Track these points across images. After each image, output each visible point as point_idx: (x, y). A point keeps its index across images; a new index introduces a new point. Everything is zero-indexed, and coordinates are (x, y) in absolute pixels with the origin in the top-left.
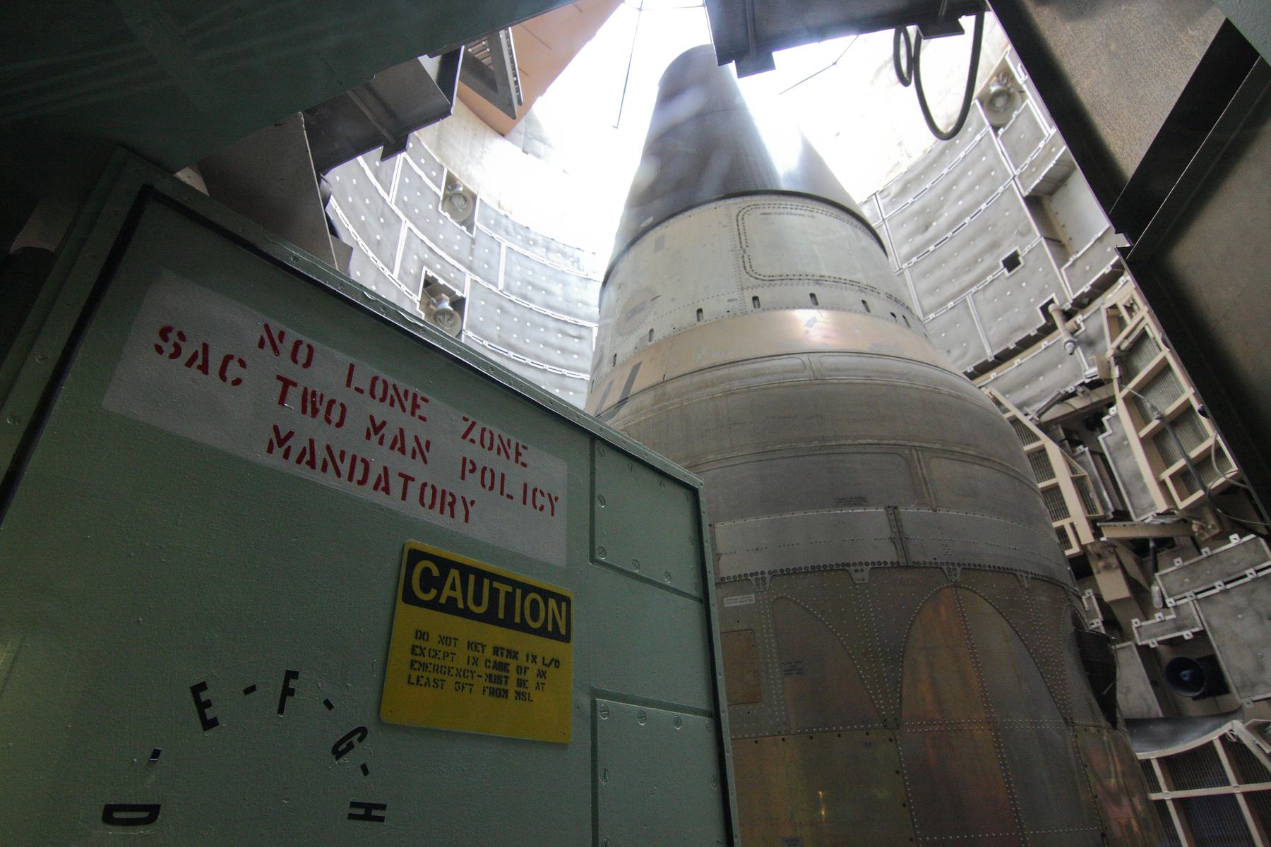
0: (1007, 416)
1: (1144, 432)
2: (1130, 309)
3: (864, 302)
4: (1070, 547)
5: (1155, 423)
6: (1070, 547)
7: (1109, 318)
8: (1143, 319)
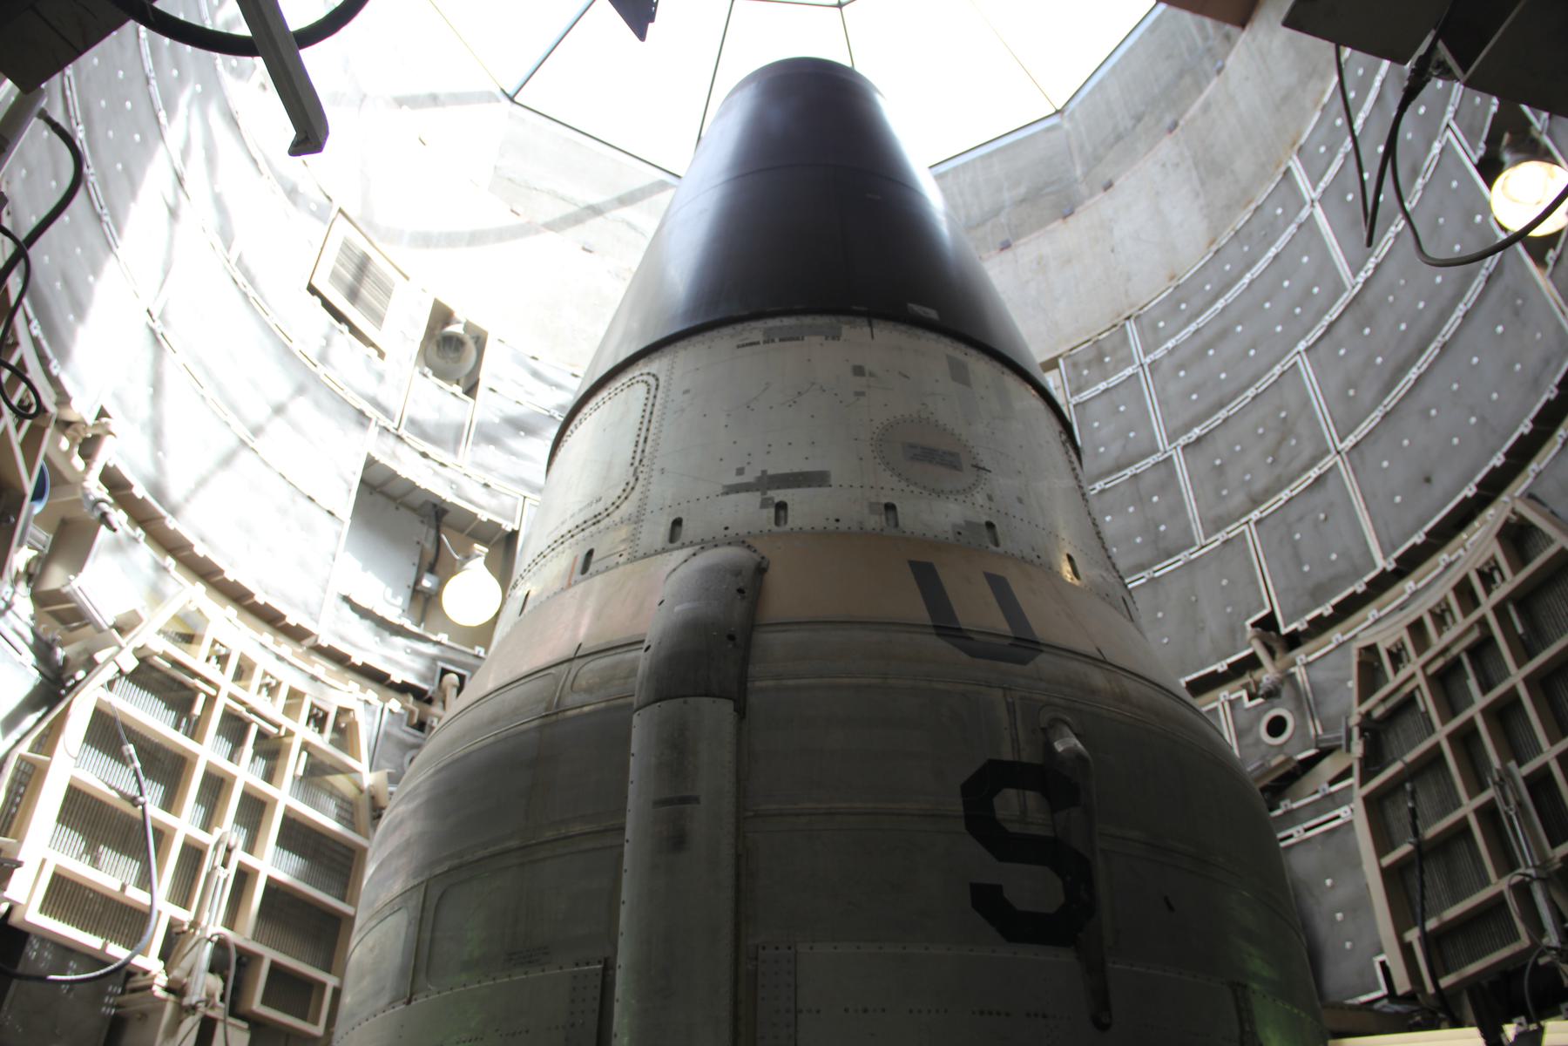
1: (1388, 860)
2: (1397, 657)
5: (1405, 849)
7: (1361, 664)
8: (1412, 676)
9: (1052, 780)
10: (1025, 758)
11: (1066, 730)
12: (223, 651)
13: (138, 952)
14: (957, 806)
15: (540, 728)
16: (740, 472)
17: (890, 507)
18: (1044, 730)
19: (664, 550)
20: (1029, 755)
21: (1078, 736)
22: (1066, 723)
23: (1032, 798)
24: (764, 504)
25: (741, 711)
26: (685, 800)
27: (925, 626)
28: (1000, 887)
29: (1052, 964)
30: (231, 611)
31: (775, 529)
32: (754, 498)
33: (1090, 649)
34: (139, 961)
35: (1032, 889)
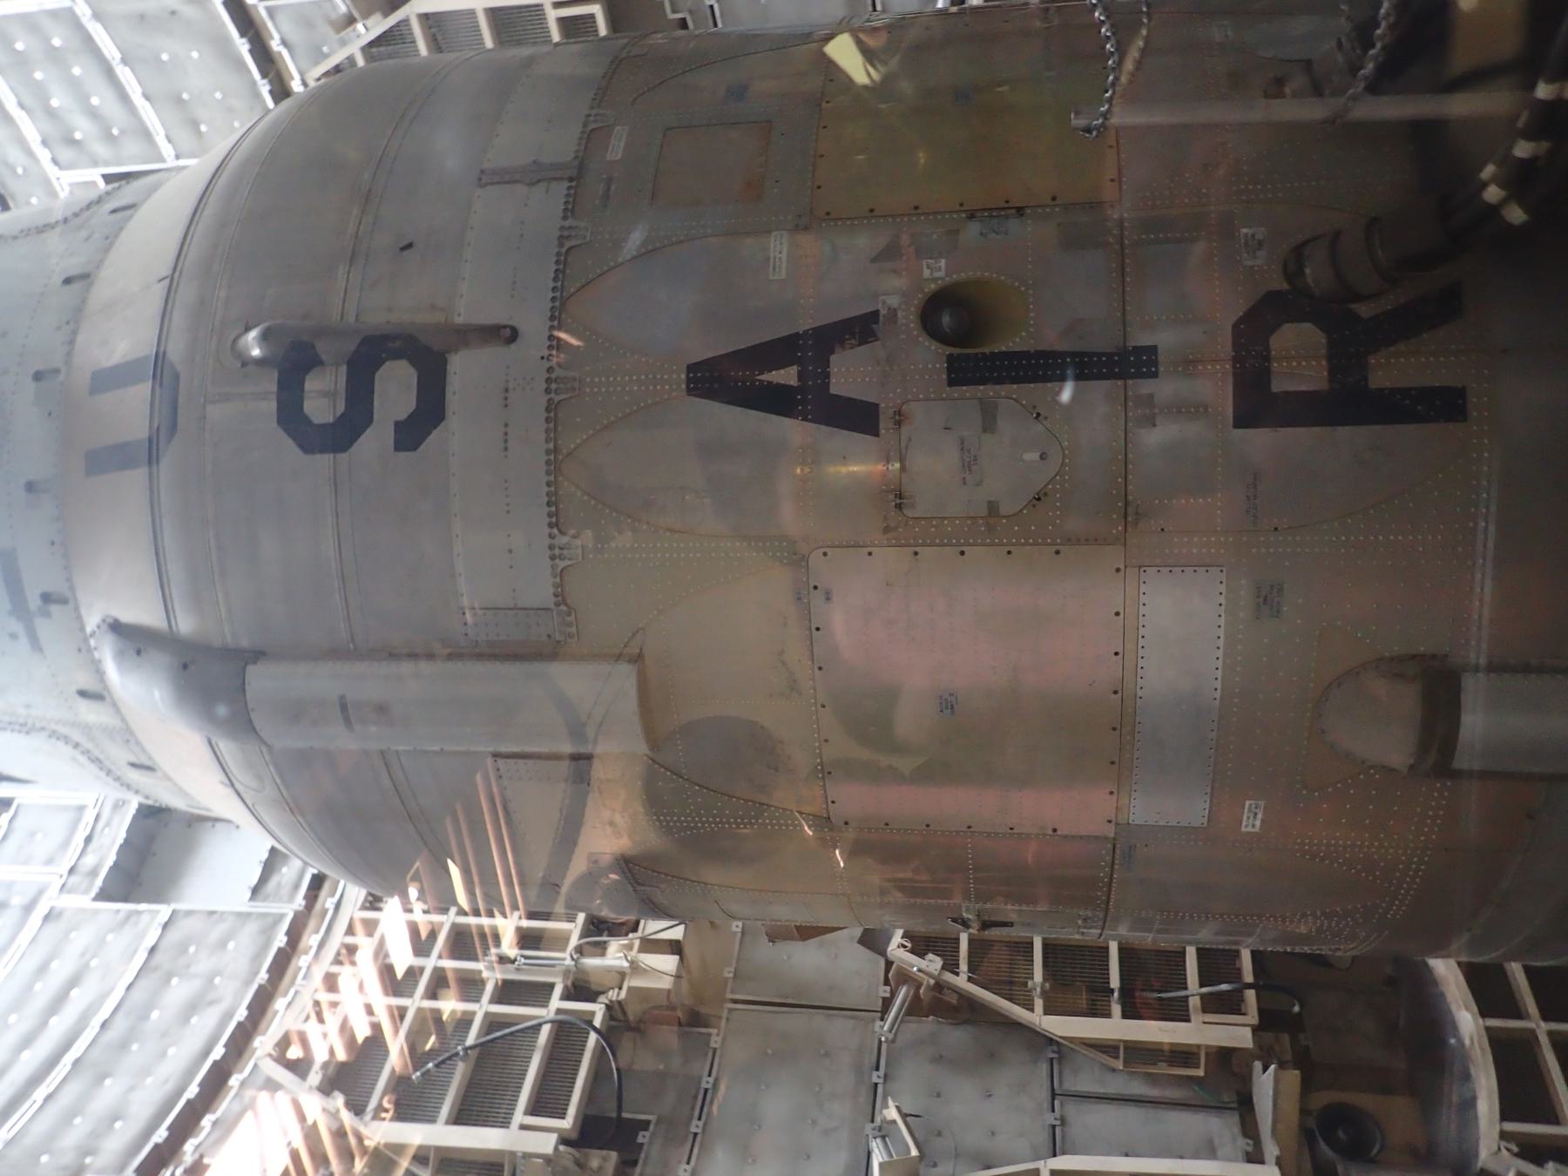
0: (361, 62)
3: (67, 281)
4: (592, 16)
6: (592, 16)
9: (294, 361)
10: (274, 388)
11: (242, 341)
12: (344, 951)
13: (590, 1023)
14: (324, 460)
15: (302, 815)
16: (14, 636)
17: (30, 487)
18: (244, 364)
19: (114, 705)
20: (269, 383)
21: (248, 329)
22: (235, 341)
23: (314, 384)
24: (47, 615)
25: (257, 655)
26: (344, 707)
27: (150, 474)
28: (397, 424)
29: (467, 371)
30: (280, 1004)
31: (71, 606)
32: (41, 625)
33: (159, 290)
34: (597, 1023)
35: (396, 389)
